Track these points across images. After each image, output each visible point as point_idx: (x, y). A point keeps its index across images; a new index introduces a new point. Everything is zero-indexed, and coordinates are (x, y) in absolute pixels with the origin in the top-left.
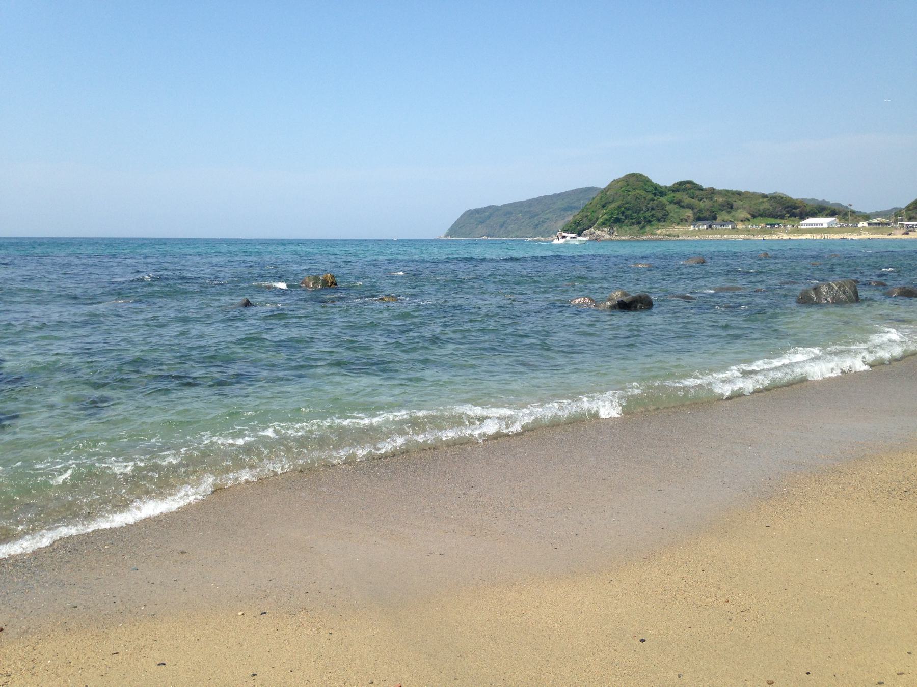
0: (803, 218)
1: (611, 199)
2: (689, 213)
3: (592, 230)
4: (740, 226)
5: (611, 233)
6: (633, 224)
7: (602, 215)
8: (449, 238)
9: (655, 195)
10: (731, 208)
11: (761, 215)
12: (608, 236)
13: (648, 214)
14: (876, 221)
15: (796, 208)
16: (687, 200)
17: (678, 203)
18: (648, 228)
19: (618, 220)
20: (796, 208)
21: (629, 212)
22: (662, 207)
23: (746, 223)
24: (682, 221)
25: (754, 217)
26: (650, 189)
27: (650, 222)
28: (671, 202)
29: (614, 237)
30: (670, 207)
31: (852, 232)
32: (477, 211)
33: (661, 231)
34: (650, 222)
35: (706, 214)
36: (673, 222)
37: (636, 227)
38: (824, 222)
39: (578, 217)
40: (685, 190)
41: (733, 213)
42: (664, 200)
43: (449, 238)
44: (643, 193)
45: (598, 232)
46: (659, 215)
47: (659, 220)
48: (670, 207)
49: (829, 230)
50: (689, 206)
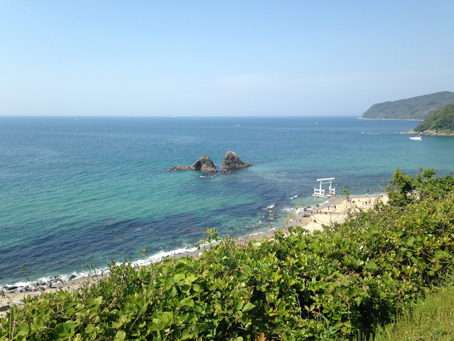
1: (438, 117)
3: (428, 131)
6: (448, 128)
7: (434, 124)
12: (435, 134)
19: (440, 127)
21: (446, 123)
29: (439, 134)
37: (449, 130)
45: (430, 132)
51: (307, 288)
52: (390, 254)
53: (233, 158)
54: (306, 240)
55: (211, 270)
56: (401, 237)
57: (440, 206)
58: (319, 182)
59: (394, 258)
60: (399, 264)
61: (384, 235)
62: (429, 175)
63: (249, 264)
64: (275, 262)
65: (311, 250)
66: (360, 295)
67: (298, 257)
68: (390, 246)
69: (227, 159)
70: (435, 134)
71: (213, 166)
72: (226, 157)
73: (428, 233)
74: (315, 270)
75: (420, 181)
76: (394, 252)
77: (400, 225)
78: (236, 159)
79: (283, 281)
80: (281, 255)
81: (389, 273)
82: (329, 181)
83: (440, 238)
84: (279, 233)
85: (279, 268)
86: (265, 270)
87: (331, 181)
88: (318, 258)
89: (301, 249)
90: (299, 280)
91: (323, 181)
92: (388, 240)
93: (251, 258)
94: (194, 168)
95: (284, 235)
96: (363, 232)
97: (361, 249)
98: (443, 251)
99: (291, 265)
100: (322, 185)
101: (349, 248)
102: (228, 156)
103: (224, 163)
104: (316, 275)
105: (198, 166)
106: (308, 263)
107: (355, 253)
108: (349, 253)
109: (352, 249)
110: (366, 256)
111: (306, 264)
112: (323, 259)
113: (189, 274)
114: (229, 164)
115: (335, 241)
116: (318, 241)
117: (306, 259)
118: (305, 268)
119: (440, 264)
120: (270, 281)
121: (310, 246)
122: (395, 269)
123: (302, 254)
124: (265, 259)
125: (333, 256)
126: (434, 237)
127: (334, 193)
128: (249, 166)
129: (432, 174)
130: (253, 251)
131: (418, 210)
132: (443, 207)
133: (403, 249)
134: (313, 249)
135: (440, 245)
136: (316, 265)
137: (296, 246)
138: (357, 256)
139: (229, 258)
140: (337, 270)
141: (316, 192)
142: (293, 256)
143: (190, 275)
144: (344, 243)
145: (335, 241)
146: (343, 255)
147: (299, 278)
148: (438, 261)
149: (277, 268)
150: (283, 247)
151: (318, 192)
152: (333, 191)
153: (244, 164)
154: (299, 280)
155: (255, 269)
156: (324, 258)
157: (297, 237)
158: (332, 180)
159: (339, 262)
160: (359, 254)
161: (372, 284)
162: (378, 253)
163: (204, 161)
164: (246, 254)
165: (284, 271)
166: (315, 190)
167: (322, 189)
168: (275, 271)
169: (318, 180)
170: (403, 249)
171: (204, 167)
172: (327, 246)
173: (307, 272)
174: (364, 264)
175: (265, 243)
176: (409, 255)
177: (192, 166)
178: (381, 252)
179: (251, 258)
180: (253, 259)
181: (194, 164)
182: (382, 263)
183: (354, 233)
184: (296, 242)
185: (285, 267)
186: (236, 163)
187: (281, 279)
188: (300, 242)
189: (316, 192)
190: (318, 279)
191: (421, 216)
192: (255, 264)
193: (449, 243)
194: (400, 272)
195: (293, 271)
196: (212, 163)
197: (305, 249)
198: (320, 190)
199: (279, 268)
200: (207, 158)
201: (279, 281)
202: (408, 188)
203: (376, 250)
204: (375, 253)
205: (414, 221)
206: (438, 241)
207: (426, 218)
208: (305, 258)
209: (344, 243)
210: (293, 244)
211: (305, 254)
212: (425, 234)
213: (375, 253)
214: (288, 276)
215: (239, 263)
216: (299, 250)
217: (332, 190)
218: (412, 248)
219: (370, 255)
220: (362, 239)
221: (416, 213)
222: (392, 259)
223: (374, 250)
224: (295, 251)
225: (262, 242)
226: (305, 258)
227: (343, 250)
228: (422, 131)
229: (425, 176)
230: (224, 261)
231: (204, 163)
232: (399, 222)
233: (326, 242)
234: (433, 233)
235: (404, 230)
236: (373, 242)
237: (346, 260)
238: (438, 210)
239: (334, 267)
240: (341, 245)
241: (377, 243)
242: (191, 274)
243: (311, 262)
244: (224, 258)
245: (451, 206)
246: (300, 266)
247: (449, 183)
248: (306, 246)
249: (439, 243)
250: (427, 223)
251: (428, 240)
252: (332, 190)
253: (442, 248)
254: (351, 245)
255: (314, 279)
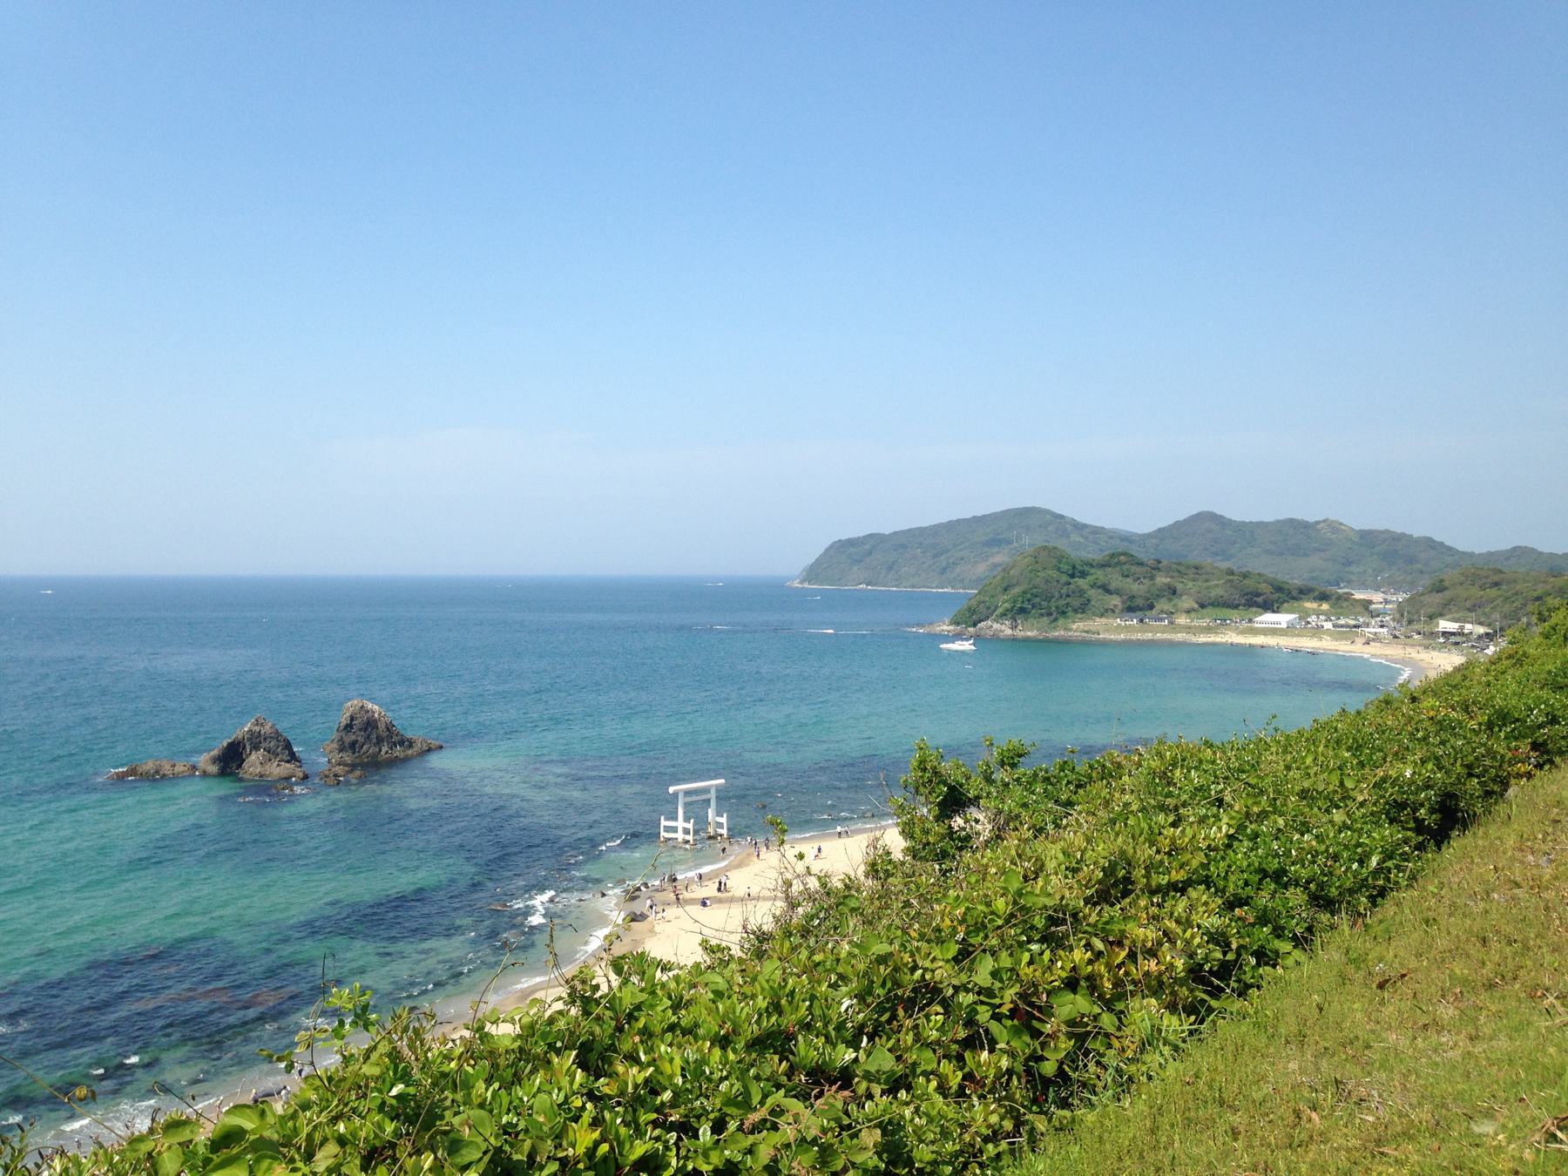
0: (1268, 607)
2: (1115, 601)
4: (1182, 620)
5: (1013, 628)
8: (806, 585)
9: (1072, 576)
10: (1174, 593)
11: (1213, 604)
12: (1009, 632)
13: (1062, 602)
14: (1342, 622)
15: (1258, 595)
16: (1116, 581)
17: (1106, 589)
18: (1061, 621)
19: (1022, 610)
20: (1258, 595)
21: (1037, 600)
22: (1082, 592)
23: (1193, 615)
24: (1106, 612)
25: (1203, 606)
26: (1065, 567)
27: (1064, 613)
28: (1093, 586)
29: (1019, 633)
30: (1092, 593)
31: (1313, 636)
32: (851, 542)
33: (1077, 627)
34: (1064, 613)
35: (1140, 602)
36: (1094, 614)
37: (1045, 620)
38: (1283, 619)
39: (974, 602)
40: (1119, 563)
41: (1176, 601)
42: (1081, 582)
43: (806, 585)
44: (1054, 574)
45: (996, 626)
46: (1076, 603)
47: (1076, 611)
48: (1092, 593)
49: (1289, 630)
50: (1118, 592)
51: (685, 1165)
52: (927, 1017)
53: (370, 724)
54: (670, 998)
55: (342, 1141)
56: (955, 959)
57: (1052, 854)
58: (676, 794)
59: (941, 1029)
60: (955, 1047)
61: (907, 958)
62: (1011, 759)
63: (482, 1106)
64: (576, 1086)
65: (691, 1031)
66: (853, 1164)
67: (649, 1058)
68: (929, 992)
69: (348, 727)
70: (1009, 632)
71: (293, 758)
72: (344, 721)
73: (1029, 941)
74: (707, 1097)
75: (989, 780)
76: (939, 1009)
77: (948, 922)
78: (381, 726)
79: (604, 1148)
80: (593, 1059)
81: (929, 1081)
82: (706, 790)
83: (1061, 953)
84: (584, 982)
85: (589, 1106)
86: (541, 1119)
87: (713, 794)
88: (717, 1052)
89: (658, 1029)
90: (657, 1139)
91: (688, 793)
92: (920, 972)
93: (488, 1082)
94: (214, 769)
95: (597, 987)
96: (843, 955)
97: (843, 1008)
98: (1075, 992)
99: (630, 1090)
100: (686, 805)
101: (810, 1008)
102: (352, 718)
103: (335, 745)
104: (712, 1116)
105: (231, 759)
106: (684, 1076)
107: (826, 1026)
108: (807, 1027)
109: (817, 1012)
110: (860, 1030)
111: (679, 1080)
112: (732, 1056)
113: (266, 1163)
114: (353, 745)
115: (763, 989)
116: (711, 996)
117: (678, 1062)
118: (676, 1094)
119: (1070, 1036)
120: (561, 1155)
121: (686, 1018)
122: (946, 1067)
123: (663, 1048)
124: (538, 1080)
125: (759, 1044)
126: (1047, 953)
127: (724, 832)
128: (429, 750)
129: (1020, 756)
130: (493, 1054)
131: (993, 870)
132: (1061, 856)
133: (966, 999)
134: (696, 1025)
135: (1064, 975)
136: (709, 1080)
137: (641, 1024)
138: (833, 1033)
139: (412, 1090)
140: (778, 1087)
141: (667, 829)
142: (632, 1058)
143: (269, 1169)
144: (792, 992)
145: (763, 989)
146: (791, 1037)
147: (657, 1132)
148: (1064, 1028)
149: (583, 1108)
150: (597, 1030)
151: (675, 830)
152: (720, 825)
153: (411, 746)
154: (657, 1139)
155: (504, 1120)
156: (735, 1051)
157: (642, 990)
158: (718, 789)
159: (781, 1062)
160: (840, 1027)
161: (890, 1122)
162: (894, 1017)
163: (256, 741)
164: (470, 1069)
165: (607, 1115)
166: (664, 823)
167: (687, 820)
168: (576, 1119)
169: (671, 790)
170: (966, 999)
171: (254, 762)
172: (743, 1010)
173: (682, 1110)
174: (856, 1060)
175: (532, 1026)
176: (984, 1015)
177: (203, 761)
178: (901, 1012)
179: (488, 1082)
180: (496, 1085)
181: (215, 752)
182: (908, 1049)
183: (817, 958)
184: (638, 1008)
185: (610, 1097)
186: (380, 741)
187: (596, 1144)
188: (652, 1006)
189: (667, 829)
190: (719, 1127)
191: (1005, 888)
192: (505, 1101)
193: (1090, 968)
194: (960, 1074)
195: (635, 1111)
196: (288, 746)
197: (672, 1028)
198: (680, 824)
199: (589, 1106)
200: (267, 729)
201: (591, 1152)
202: (954, 801)
203: (884, 1010)
204: (883, 1019)
205: (988, 904)
206: (1059, 964)
207: (1019, 893)
208: (671, 1060)
209: (792, 992)
210: (631, 1017)
211: (670, 1045)
212: (1021, 944)
213: (883, 1019)
214: (623, 1130)
215: (448, 1103)
216: (651, 1035)
217: (719, 819)
218: (989, 993)
219: (870, 1029)
220: (841, 977)
221: (990, 877)
222: (934, 1034)
223: (881, 1009)
224: (637, 1039)
225: (526, 1020)
226: (673, 1057)
227: (789, 1020)
228: (975, 625)
229: (1002, 764)
230: (394, 1102)
231: (256, 748)
232: (947, 913)
233: (735, 997)
234: (1041, 941)
235: (960, 936)
236: (877, 981)
237: (802, 1053)
238: (1051, 865)
239: (768, 1080)
240: (783, 1002)
241: (889, 985)
242: (275, 1165)
243: (694, 1071)
244: (394, 1092)
245: (1083, 852)
246: (655, 1093)
247: (1069, 783)
248: (674, 1019)
249: (1061, 971)
250: (1022, 908)
251: (1031, 963)
252: (719, 819)
253: (1071, 984)
254: (813, 998)
255: (705, 1132)
